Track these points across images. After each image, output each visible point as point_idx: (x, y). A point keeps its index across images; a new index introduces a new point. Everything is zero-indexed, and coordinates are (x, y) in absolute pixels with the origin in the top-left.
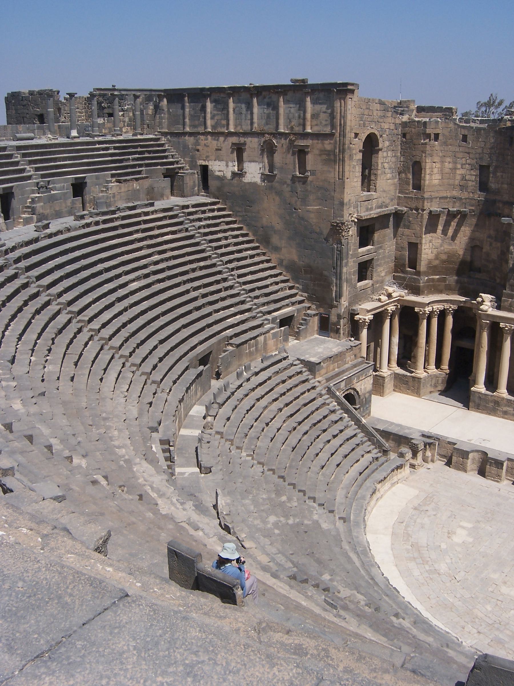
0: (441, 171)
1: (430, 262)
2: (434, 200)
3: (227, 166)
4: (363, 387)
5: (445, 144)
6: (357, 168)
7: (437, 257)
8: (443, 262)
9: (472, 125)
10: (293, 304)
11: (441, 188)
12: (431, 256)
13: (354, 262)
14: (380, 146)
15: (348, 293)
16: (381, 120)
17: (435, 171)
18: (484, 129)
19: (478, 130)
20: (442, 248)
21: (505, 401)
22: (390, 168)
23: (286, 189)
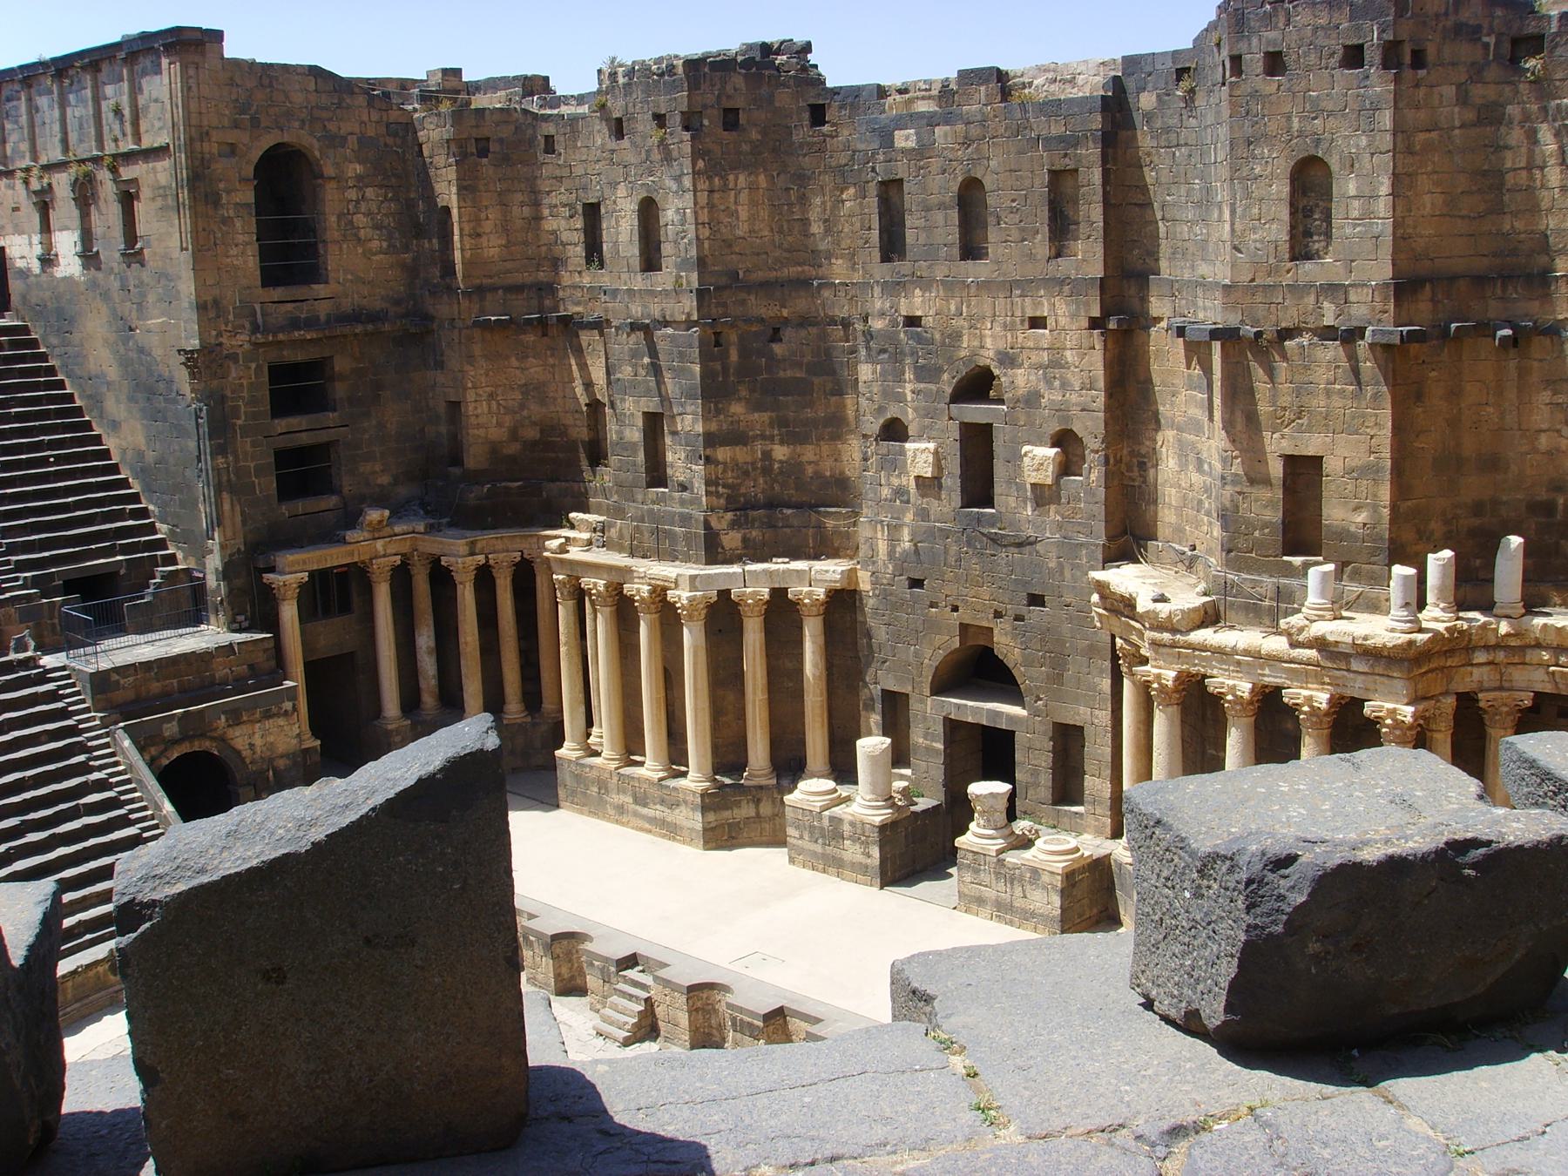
0: (505, 228)
1: (494, 449)
2: (489, 296)
3: (30, 244)
4: (258, 741)
5: (506, 160)
6: (238, 224)
7: (514, 434)
8: (532, 445)
9: (565, 110)
10: (125, 550)
11: (509, 265)
12: (496, 434)
13: (254, 444)
14: (329, 171)
15: (238, 519)
16: (325, 115)
17: (488, 226)
18: (584, 117)
19: (574, 119)
20: (525, 413)
21: (615, 779)
22: (377, 227)
23: (115, 285)
